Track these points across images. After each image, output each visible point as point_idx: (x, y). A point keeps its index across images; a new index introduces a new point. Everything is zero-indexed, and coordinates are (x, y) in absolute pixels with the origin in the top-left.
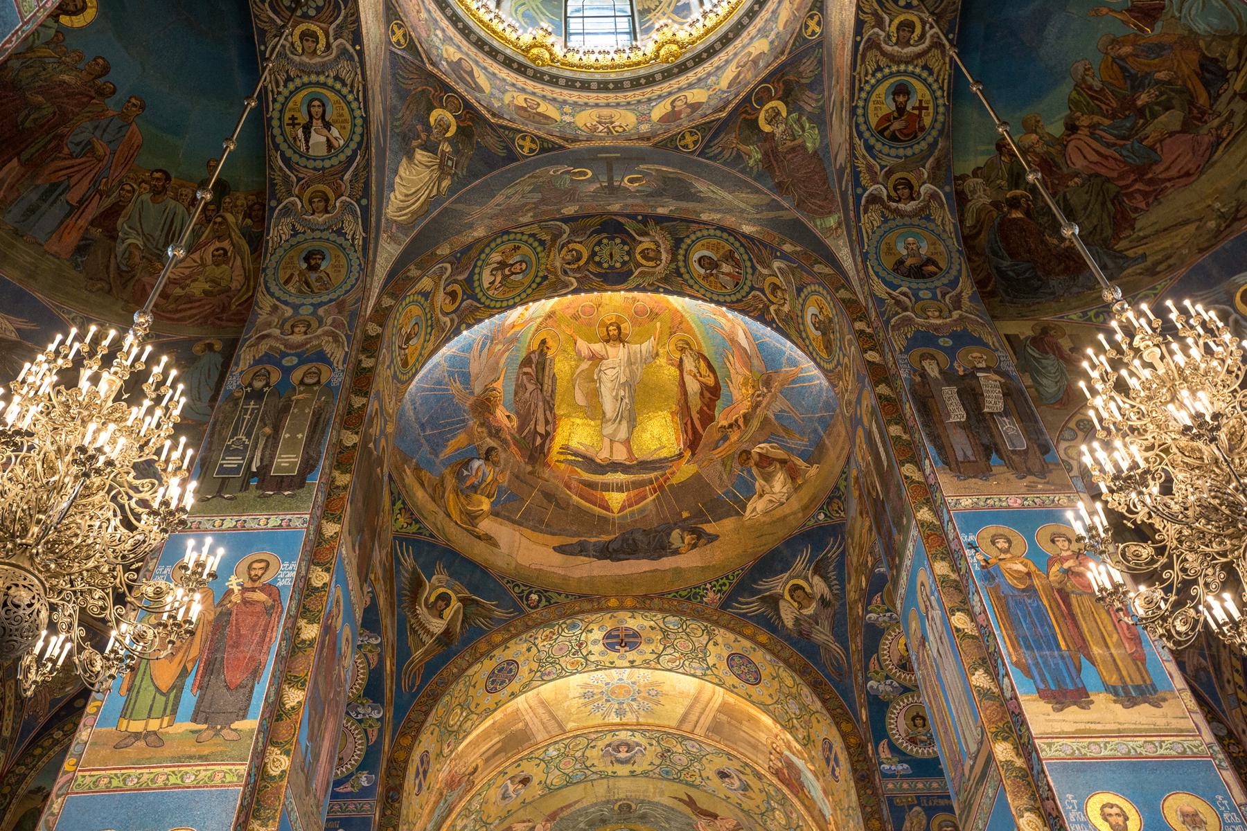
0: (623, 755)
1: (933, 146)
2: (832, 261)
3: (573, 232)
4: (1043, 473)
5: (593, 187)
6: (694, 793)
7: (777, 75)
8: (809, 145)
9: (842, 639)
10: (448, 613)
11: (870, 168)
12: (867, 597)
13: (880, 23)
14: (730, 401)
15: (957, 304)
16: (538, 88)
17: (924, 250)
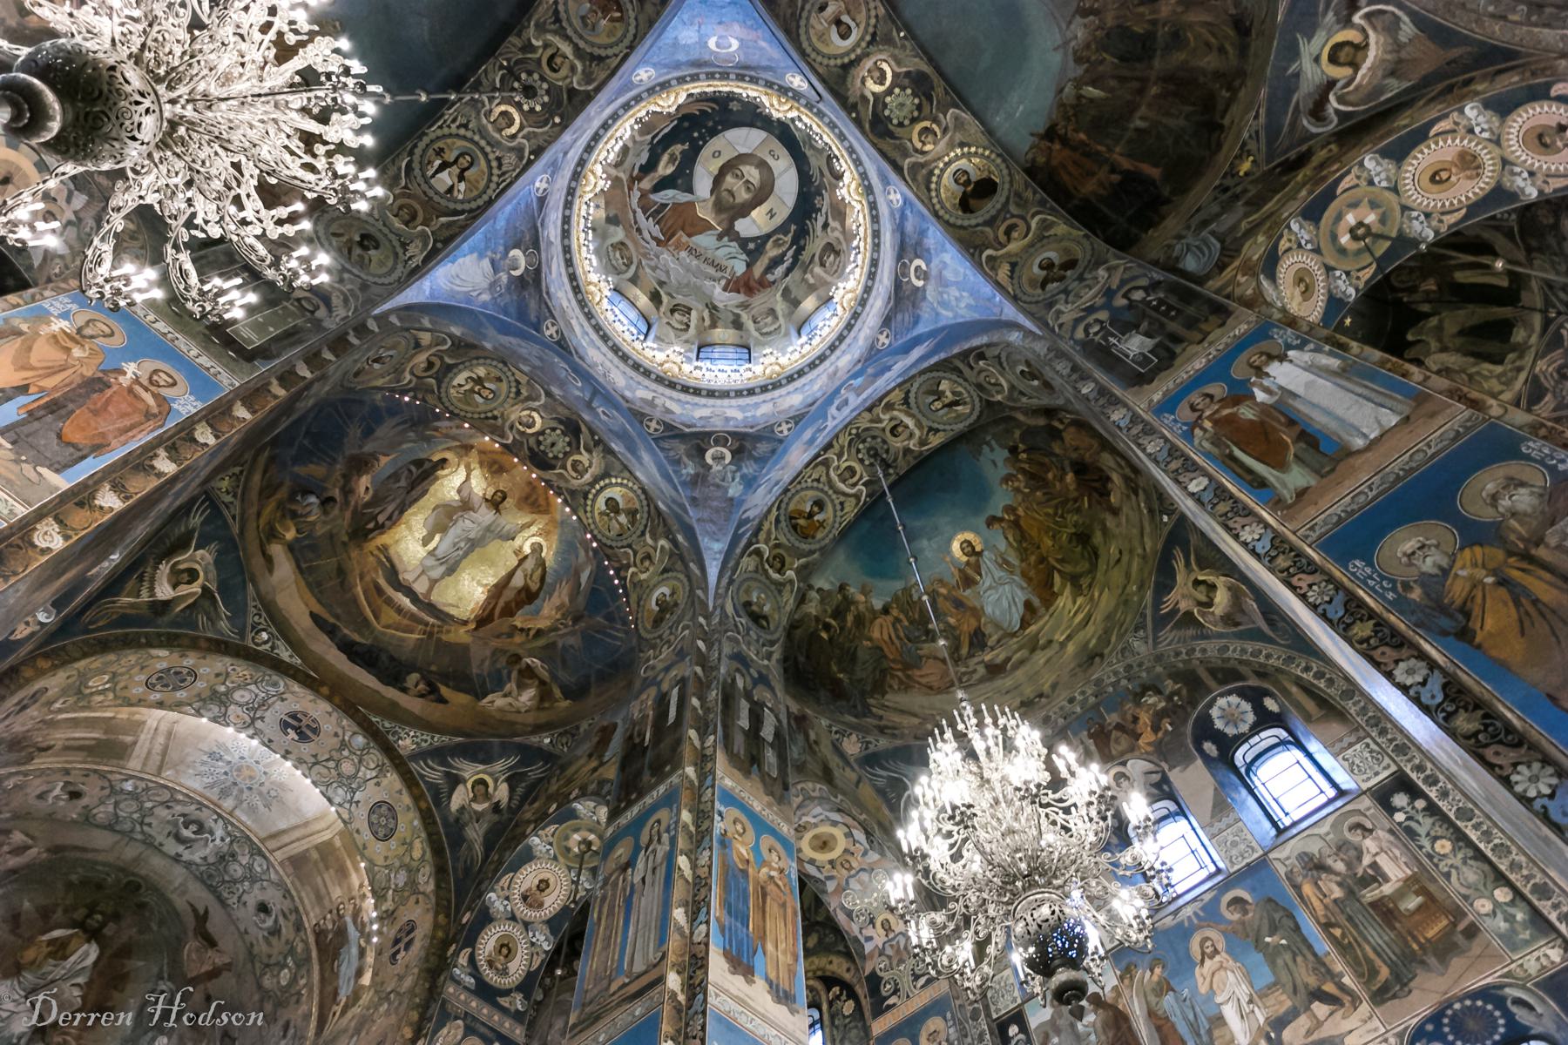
1: (812, 552)
2: (703, 568)
3: (544, 406)
5: (578, 393)
11: (769, 533)
13: (840, 456)
15: (769, 656)
17: (766, 609)
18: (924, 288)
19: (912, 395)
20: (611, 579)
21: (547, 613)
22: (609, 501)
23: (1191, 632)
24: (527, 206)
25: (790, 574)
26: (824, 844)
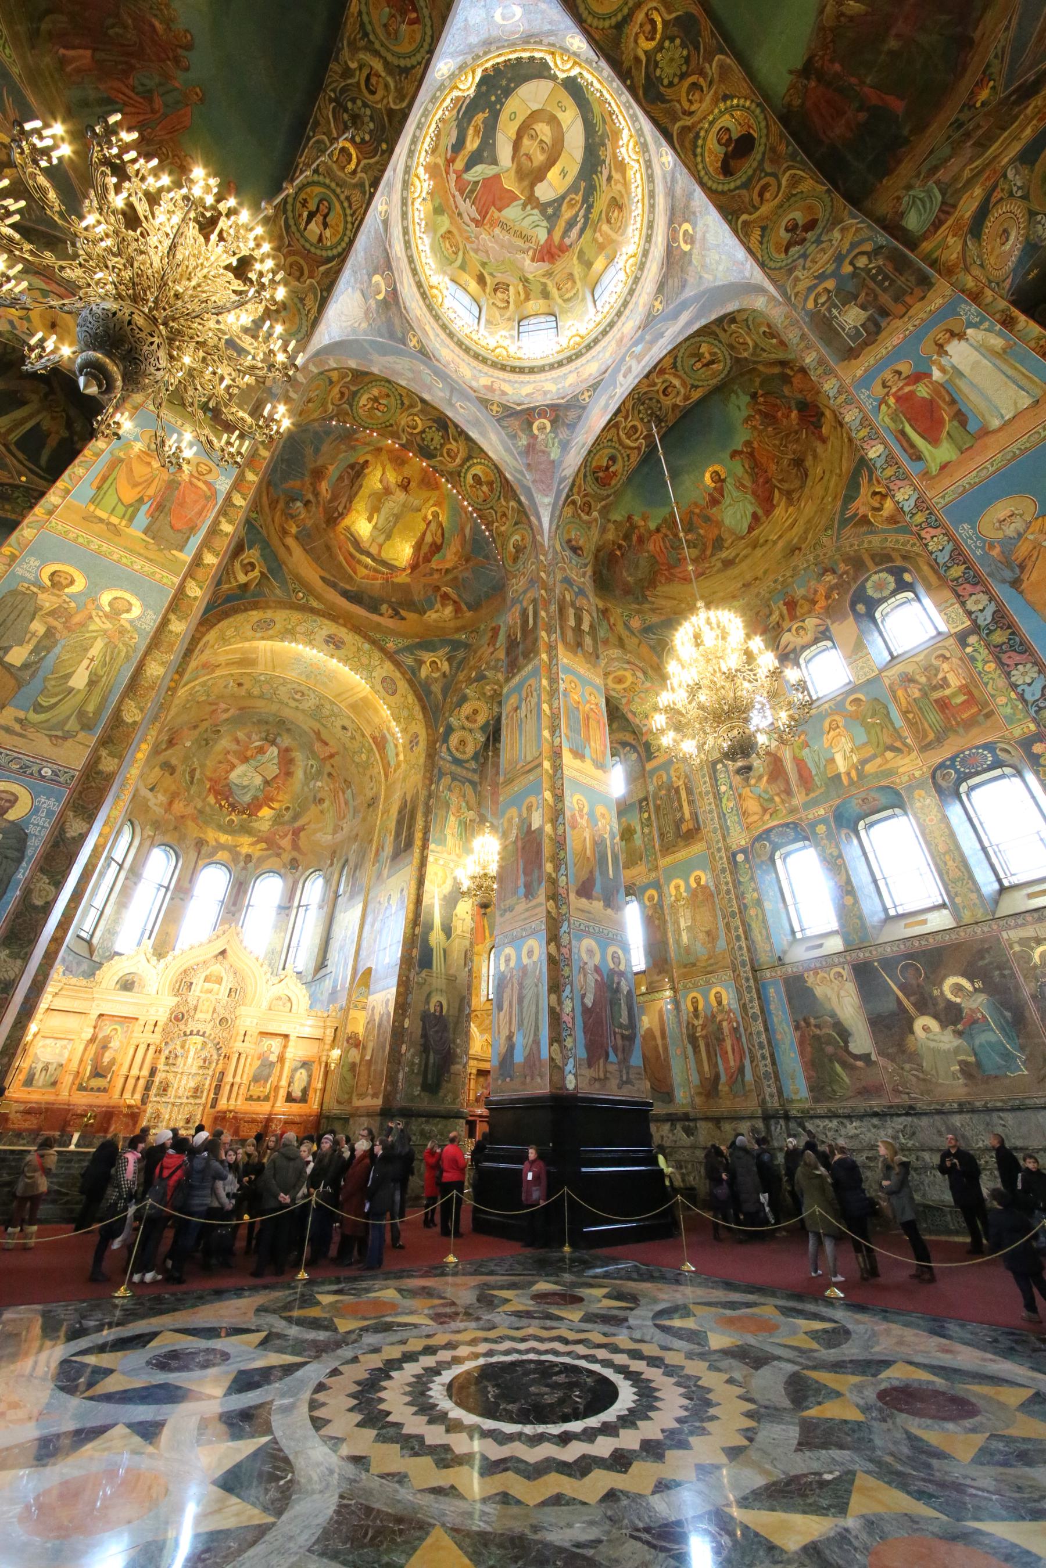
0: (297, 697)
1: (608, 496)
2: (540, 521)
3: (421, 411)
4: (594, 666)
5: (441, 394)
6: (322, 729)
7: (554, 407)
8: (553, 456)
9: (445, 692)
10: (251, 575)
11: (580, 487)
12: (470, 681)
13: (626, 418)
14: (443, 560)
15: (584, 575)
16: (428, 315)
17: (581, 543)
18: (689, 254)
19: (679, 360)
20: (483, 532)
21: (449, 557)
22: (475, 476)
23: (865, 529)
24: (376, 231)
25: (595, 514)
26: (620, 680)
